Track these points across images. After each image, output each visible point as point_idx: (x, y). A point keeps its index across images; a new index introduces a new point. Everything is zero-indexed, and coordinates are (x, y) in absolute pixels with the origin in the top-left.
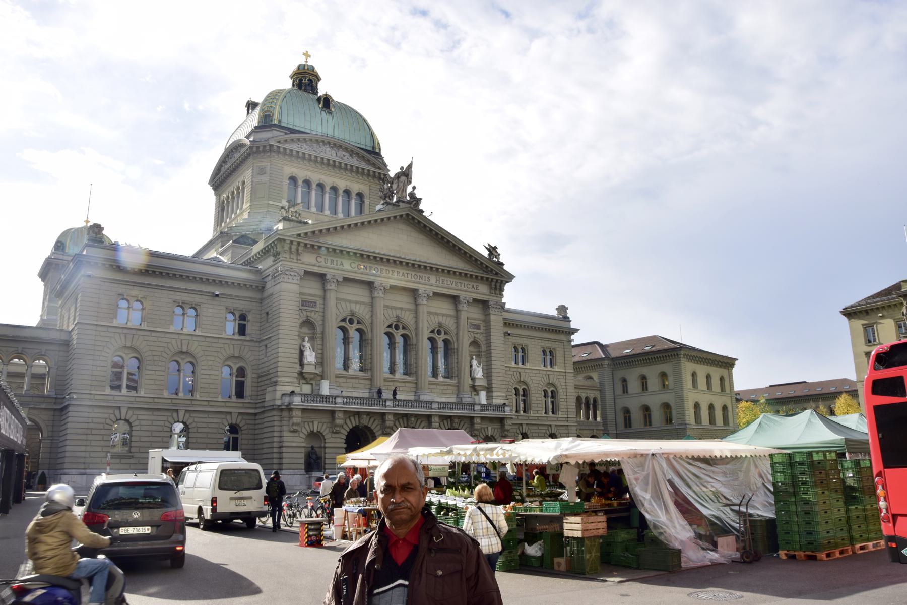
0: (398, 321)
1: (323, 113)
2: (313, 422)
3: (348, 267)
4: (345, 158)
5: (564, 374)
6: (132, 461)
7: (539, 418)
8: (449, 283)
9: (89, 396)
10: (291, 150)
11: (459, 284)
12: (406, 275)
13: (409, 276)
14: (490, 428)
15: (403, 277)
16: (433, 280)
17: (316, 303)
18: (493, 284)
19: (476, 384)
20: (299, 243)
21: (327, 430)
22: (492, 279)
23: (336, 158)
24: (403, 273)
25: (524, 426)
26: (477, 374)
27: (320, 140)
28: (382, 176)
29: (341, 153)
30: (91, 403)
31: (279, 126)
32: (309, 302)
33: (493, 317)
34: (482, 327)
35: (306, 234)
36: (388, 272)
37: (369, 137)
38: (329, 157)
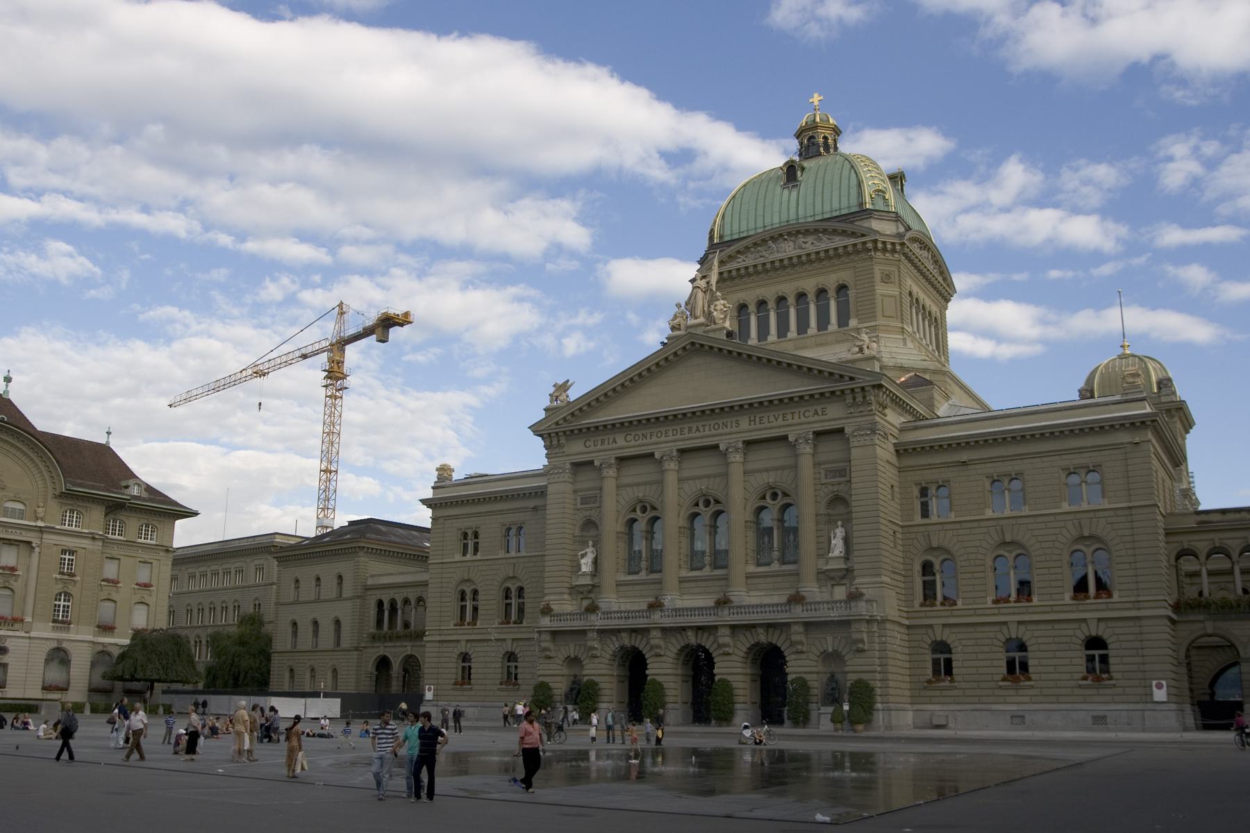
0: (704, 495)
1: (786, 192)
2: (568, 645)
3: (625, 444)
4: (807, 245)
5: (1127, 512)
6: (472, 693)
7: (1055, 608)
8: (772, 419)
9: (438, 632)
10: (730, 272)
11: (789, 416)
12: (701, 429)
13: (707, 428)
14: (830, 639)
15: (698, 434)
16: (744, 423)
17: (596, 497)
18: (849, 400)
19: (825, 568)
20: (557, 433)
21: (586, 653)
22: (842, 391)
23: (794, 252)
24: (698, 427)
25: (1013, 628)
26: (833, 553)
27: (767, 237)
28: (870, 245)
29: (801, 239)
30: (438, 638)
31: (723, 244)
32: (590, 498)
33: (855, 453)
34: (848, 472)
35: (564, 419)
36: (675, 432)
37: (854, 192)
38: (788, 254)
